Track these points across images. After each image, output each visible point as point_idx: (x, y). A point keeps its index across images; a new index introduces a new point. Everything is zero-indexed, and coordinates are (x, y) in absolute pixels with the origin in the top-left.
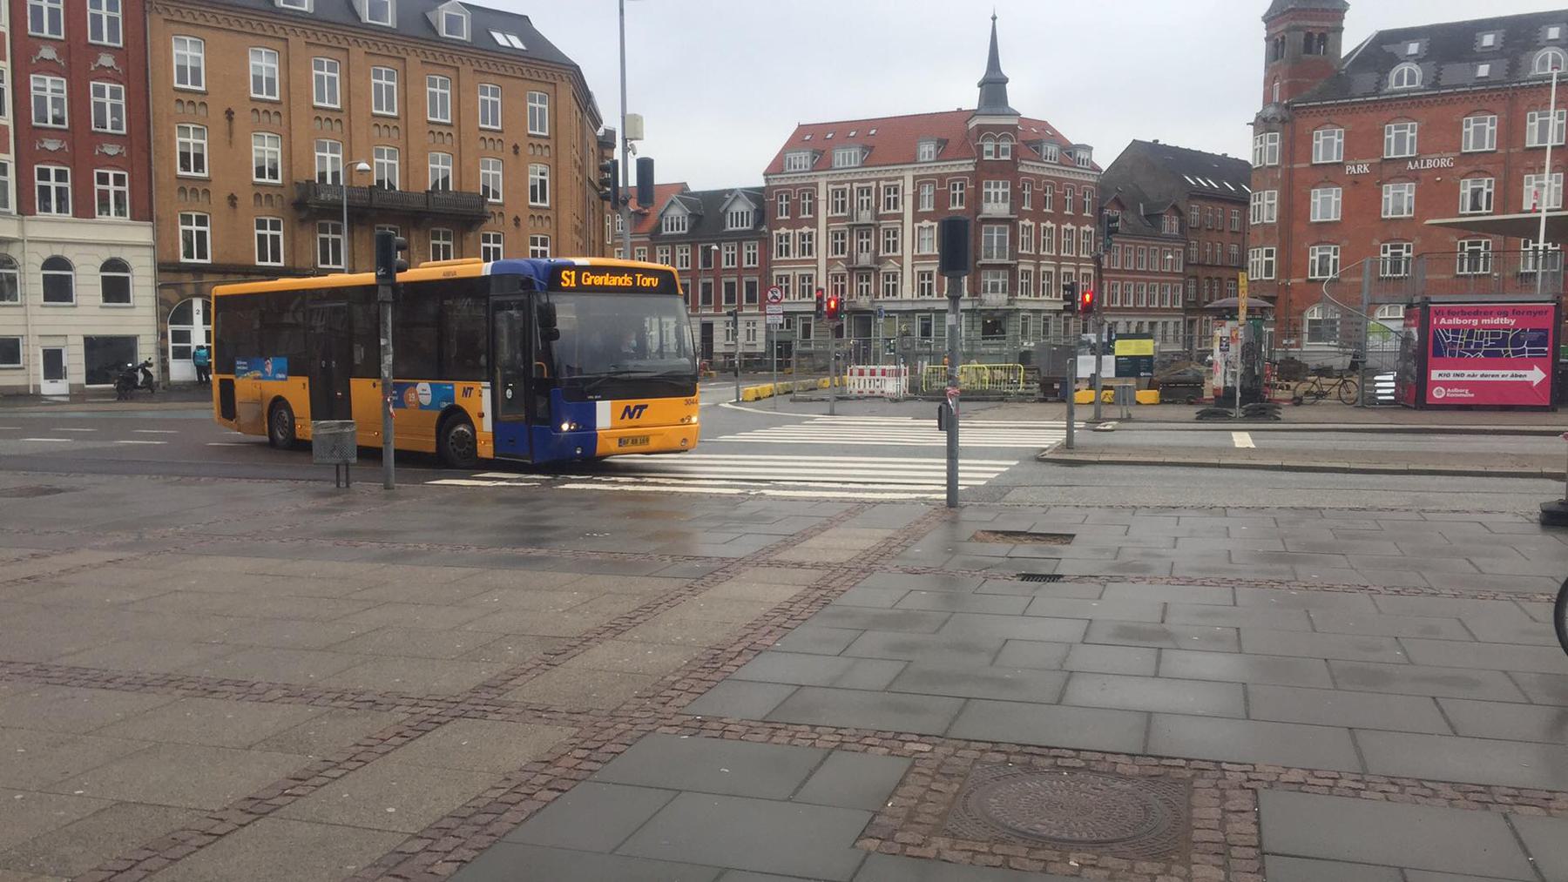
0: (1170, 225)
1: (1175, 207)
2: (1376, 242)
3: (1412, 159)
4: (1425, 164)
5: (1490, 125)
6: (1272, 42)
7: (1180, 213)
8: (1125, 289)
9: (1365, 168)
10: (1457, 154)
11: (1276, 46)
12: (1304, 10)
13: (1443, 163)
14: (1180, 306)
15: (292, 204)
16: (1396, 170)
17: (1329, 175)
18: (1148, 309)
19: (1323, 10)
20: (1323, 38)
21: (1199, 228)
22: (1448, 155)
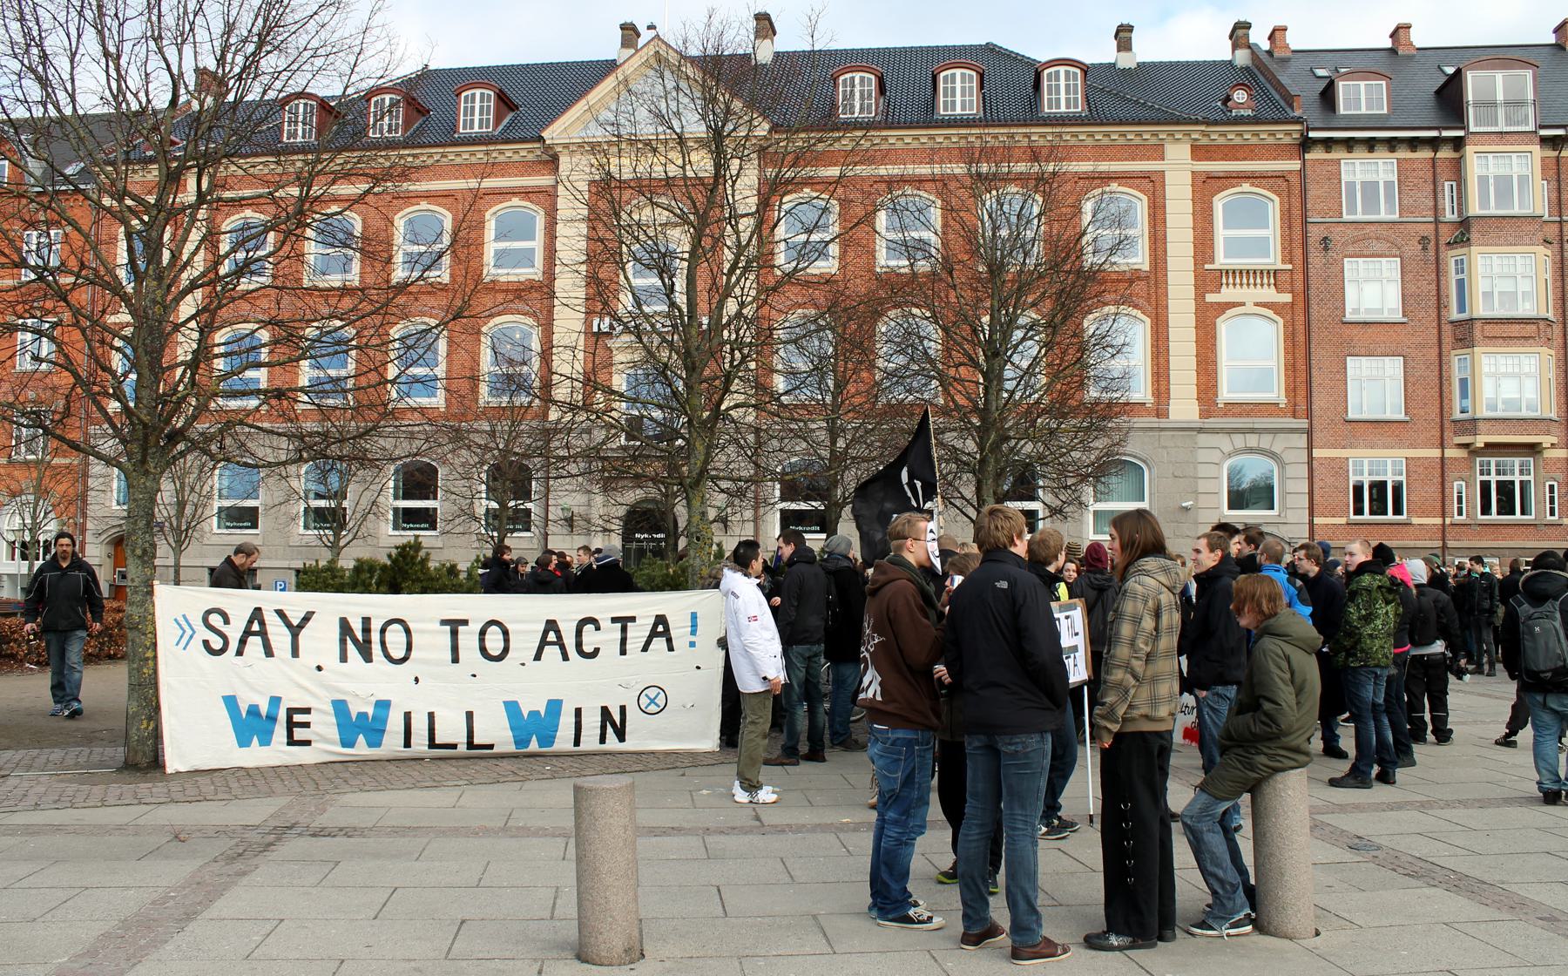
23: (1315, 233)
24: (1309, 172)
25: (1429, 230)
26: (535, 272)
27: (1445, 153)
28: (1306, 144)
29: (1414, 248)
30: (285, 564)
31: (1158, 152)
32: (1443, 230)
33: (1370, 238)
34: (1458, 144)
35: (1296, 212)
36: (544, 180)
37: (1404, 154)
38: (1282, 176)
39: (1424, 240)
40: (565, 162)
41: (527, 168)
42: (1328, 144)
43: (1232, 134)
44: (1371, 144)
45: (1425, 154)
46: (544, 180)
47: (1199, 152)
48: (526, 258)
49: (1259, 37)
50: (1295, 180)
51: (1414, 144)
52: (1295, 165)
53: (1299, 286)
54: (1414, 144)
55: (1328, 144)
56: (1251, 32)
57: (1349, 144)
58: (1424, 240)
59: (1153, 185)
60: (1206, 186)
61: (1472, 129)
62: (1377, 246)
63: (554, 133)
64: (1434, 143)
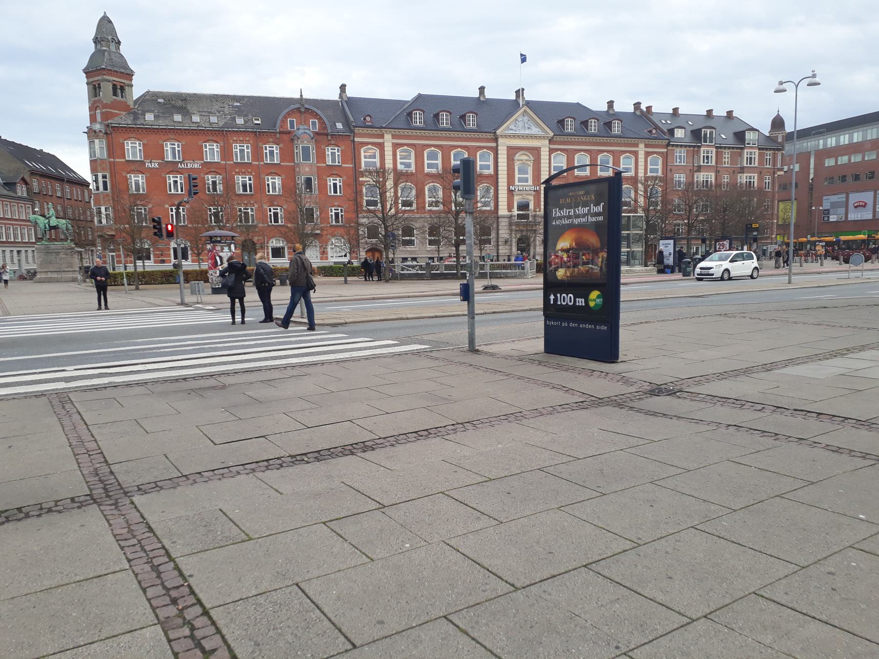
0: (21, 191)
1: (23, 179)
2: (167, 206)
3: (181, 162)
4: (187, 166)
5: (216, 147)
6: (91, 86)
7: (26, 183)
8: (7, 229)
9: (156, 165)
10: (202, 162)
11: (95, 88)
12: (111, 70)
13: (196, 166)
14: (34, 241)
15: (734, 133)
16: (172, 167)
17: (137, 167)
18: (15, 242)
19: (115, 71)
20: (122, 89)
21: (39, 193)
22: (199, 162)
23: (669, 168)
24: (668, 152)
25: (691, 168)
26: (491, 171)
27: (696, 149)
28: (668, 145)
29: (688, 172)
30: (426, 256)
32: (695, 168)
33: (680, 169)
34: (699, 147)
35: (665, 162)
36: (494, 145)
37: (687, 148)
38: (662, 153)
39: (690, 170)
40: (500, 141)
41: (488, 140)
42: (673, 145)
43: (653, 142)
44: (681, 146)
45: (692, 149)
46: (494, 145)
47: (646, 146)
48: (488, 167)
49: (643, 107)
50: (665, 154)
52: (665, 150)
54: (690, 146)
55: (673, 145)
56: (641, 105)
57: (677, 146)
58: (690, 170)
59: (636, 154)
60: (647, 154)
61: (703, 144)
62: (681, 171)
63: (498, 132)
64: (694, 146)
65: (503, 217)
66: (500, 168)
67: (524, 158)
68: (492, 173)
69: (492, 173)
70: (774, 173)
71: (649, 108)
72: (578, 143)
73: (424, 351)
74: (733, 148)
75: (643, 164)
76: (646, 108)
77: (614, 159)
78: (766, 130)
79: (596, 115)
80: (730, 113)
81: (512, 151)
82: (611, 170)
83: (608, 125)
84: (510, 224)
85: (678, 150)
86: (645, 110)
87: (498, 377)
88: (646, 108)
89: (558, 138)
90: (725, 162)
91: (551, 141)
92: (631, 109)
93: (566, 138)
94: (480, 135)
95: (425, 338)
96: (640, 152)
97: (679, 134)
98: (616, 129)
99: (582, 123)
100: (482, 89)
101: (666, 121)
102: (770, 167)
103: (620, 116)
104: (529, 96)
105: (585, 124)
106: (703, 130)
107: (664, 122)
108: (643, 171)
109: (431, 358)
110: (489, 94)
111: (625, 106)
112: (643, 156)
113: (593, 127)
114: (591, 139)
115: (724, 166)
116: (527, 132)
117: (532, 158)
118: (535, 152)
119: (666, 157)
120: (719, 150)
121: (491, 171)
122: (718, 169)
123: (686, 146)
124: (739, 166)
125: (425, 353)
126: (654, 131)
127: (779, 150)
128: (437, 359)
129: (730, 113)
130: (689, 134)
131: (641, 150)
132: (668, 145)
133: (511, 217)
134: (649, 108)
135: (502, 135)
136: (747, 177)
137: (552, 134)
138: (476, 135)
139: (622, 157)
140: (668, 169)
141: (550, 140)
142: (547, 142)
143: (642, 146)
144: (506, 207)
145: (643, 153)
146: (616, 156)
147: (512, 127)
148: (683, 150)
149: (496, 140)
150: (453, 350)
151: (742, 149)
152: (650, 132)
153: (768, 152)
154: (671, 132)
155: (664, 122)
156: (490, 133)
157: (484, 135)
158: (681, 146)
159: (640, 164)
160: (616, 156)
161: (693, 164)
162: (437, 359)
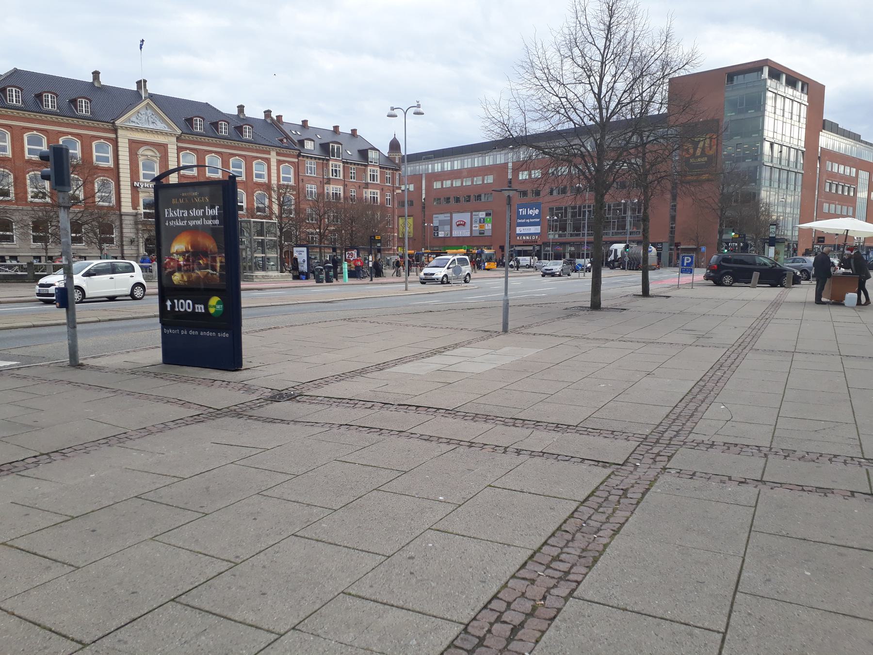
15: (320, 144)
23: (301, 178)
24: (300, 164)
25: (322, 180)
27: (325, 162)
28: (299, 155)
29: (319, 184)
30: (30, 254)
31: (269, 153)
32: (325, 180)
33: (311, 180)
34: (328, 160)
35: (297, 171)
37: (317, 161)
38: (294, 162)
40: (120, 132)
42: (303, 156)
43: (285, 151)
44: (311, 158)
45: (321, 161)
46: (113, 136)
47: (278, 154)
48: (106, 160)
50: (296, 164)
51: (319, 159)
52: (297, 160)
53: (297, 191)
54: (319, 159)
55: (303, 156)
57: (307, 157)
59: (268, 161)
60: (279, 162)
62: (312, 182)
63: (118, 123)
64: (323, 159)
65: (127, 215)
66: (121, 162)
67: (149, 153)
68: (112, 166)
69: (112, 166)
70: (393, 191)
71: (279, 117)
72: (208, 145)
73: (10, 369)
74: (358, 164)
75: (276, 171)
76: (277, 116)
77: (246, 164)
78: (385, 151)
79: (227, 118)
80: (354, 131)
81: (134, 145)
82: (220, 172)
83: (239, 129)
84: (136, 223)
85: (309, 161)
86: (275, 118)
87: (104, 394)
88: (277, 116)
89: (187, 137)
90: (351, 177)
91: (179, 139)
92: (262, 116)
93: (195, 138)
94: (96, 124)
95: (14, 352)
96: (272, 160)
97: (309, 145)
98: (247, 135)
99: (212, 124)
100: (96, 74)
101: (296, 131)
102: (390, 185)
103: (251, 122)
104: (152, 88)
105: (215, 125)
106: (331, 144)
107: (294, 133)
108: (276, 179)
109: (18, 377)
110: (104, 81)
111: (255, 112)
112: (275, 164)
113: (224, 129)
114: (222, 142)
115: (351, 180)
116: (151, 126)
117: (158, 155)
118: (162, 148)
119: (297, 167)
120: (346, 165)
121: (111, 164)
122: (346, 183)
123: (315, 158)
124: (364, 182)
125: (11, 372)
126: (285, 141)
127: (397, 170)
128: (25, 377)
129: (354, 131)
130: (318, 146)
131: (273, 157)
132: (299, 155)
133: (136, 215)
134: (279, 117)
135: (121, 127)
136: (371, 192)
137: (179, 132)
138: (91, 123)
139: (254, 163)
140: (300, 179)
141: (177, 138)
142: (174, 139)
143: (273, 154)
144: (130, 204)
145: (275, 160)
146: (249, 161)
147: (134, 119)
148: (313, 161)
149: (115, 130)
150: (49, 366)
151: (366, 166)
152: (281, 141)
153: (388, 171)
154: (301, 143)
155: (294, 133)
156: (108, 122)
157: (101, 125)
158: (311, 158)
159: (272, 171)
160: (249, 161)
161: (323, 176)
162: (25, 377)
